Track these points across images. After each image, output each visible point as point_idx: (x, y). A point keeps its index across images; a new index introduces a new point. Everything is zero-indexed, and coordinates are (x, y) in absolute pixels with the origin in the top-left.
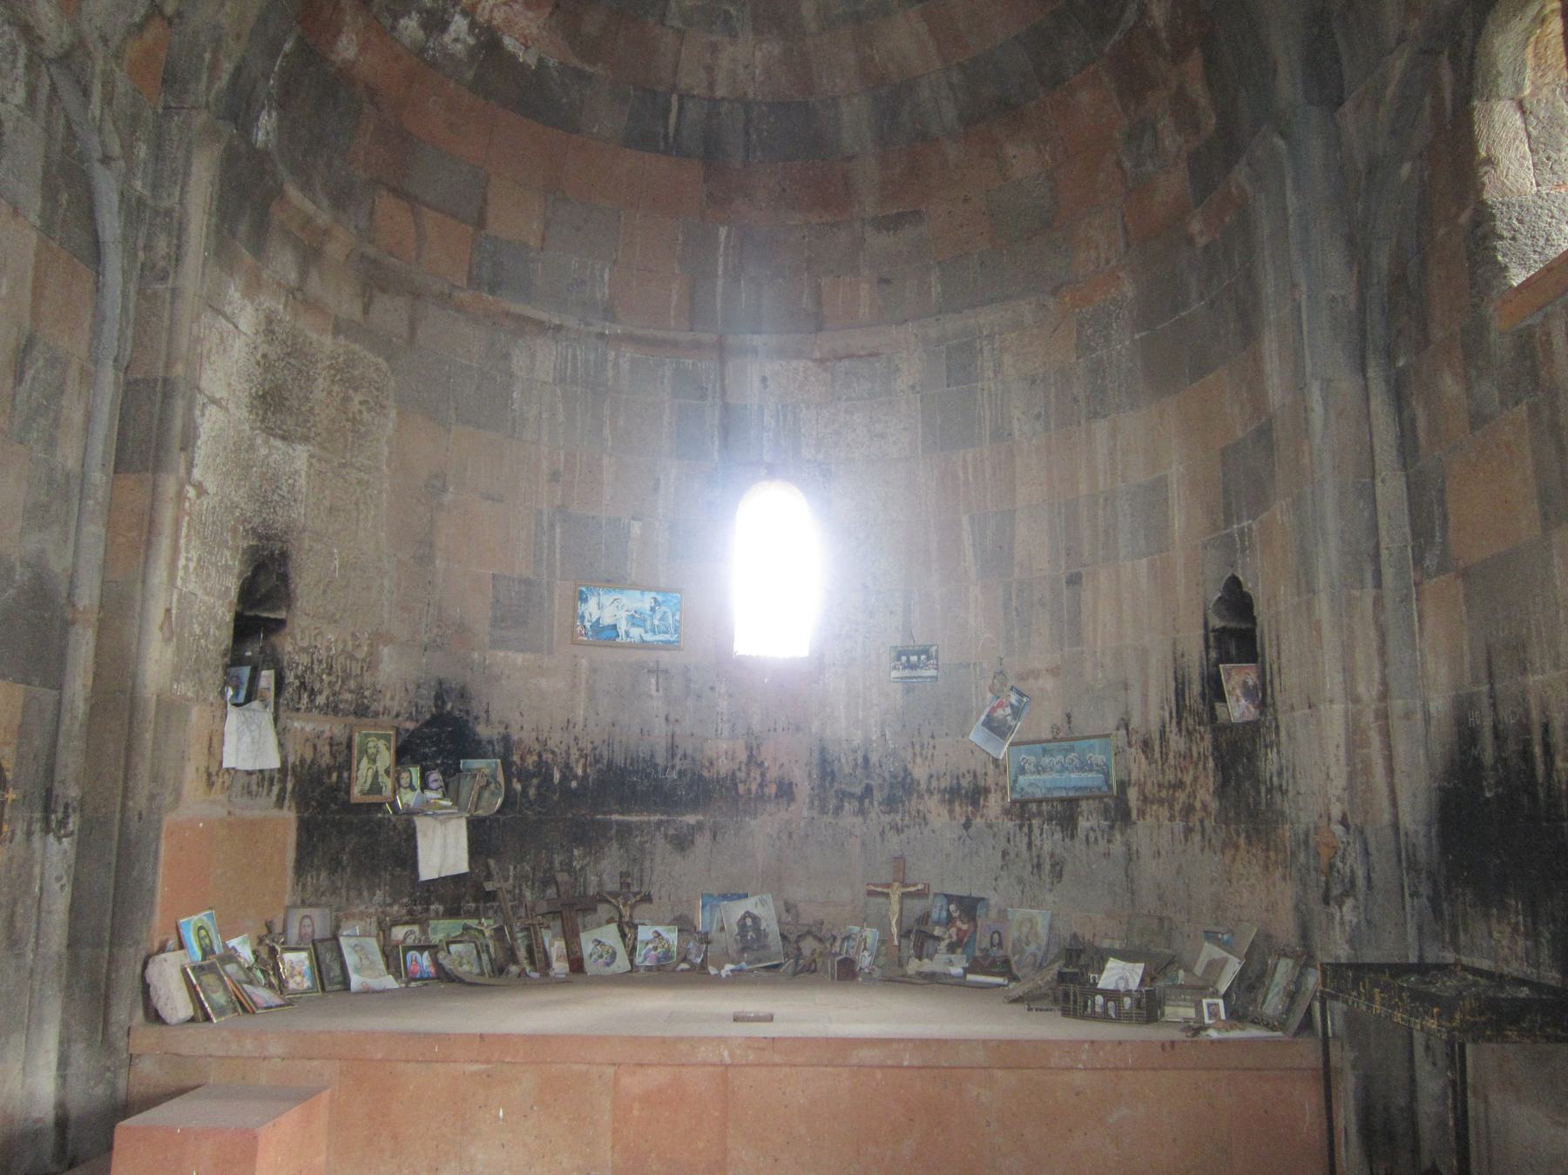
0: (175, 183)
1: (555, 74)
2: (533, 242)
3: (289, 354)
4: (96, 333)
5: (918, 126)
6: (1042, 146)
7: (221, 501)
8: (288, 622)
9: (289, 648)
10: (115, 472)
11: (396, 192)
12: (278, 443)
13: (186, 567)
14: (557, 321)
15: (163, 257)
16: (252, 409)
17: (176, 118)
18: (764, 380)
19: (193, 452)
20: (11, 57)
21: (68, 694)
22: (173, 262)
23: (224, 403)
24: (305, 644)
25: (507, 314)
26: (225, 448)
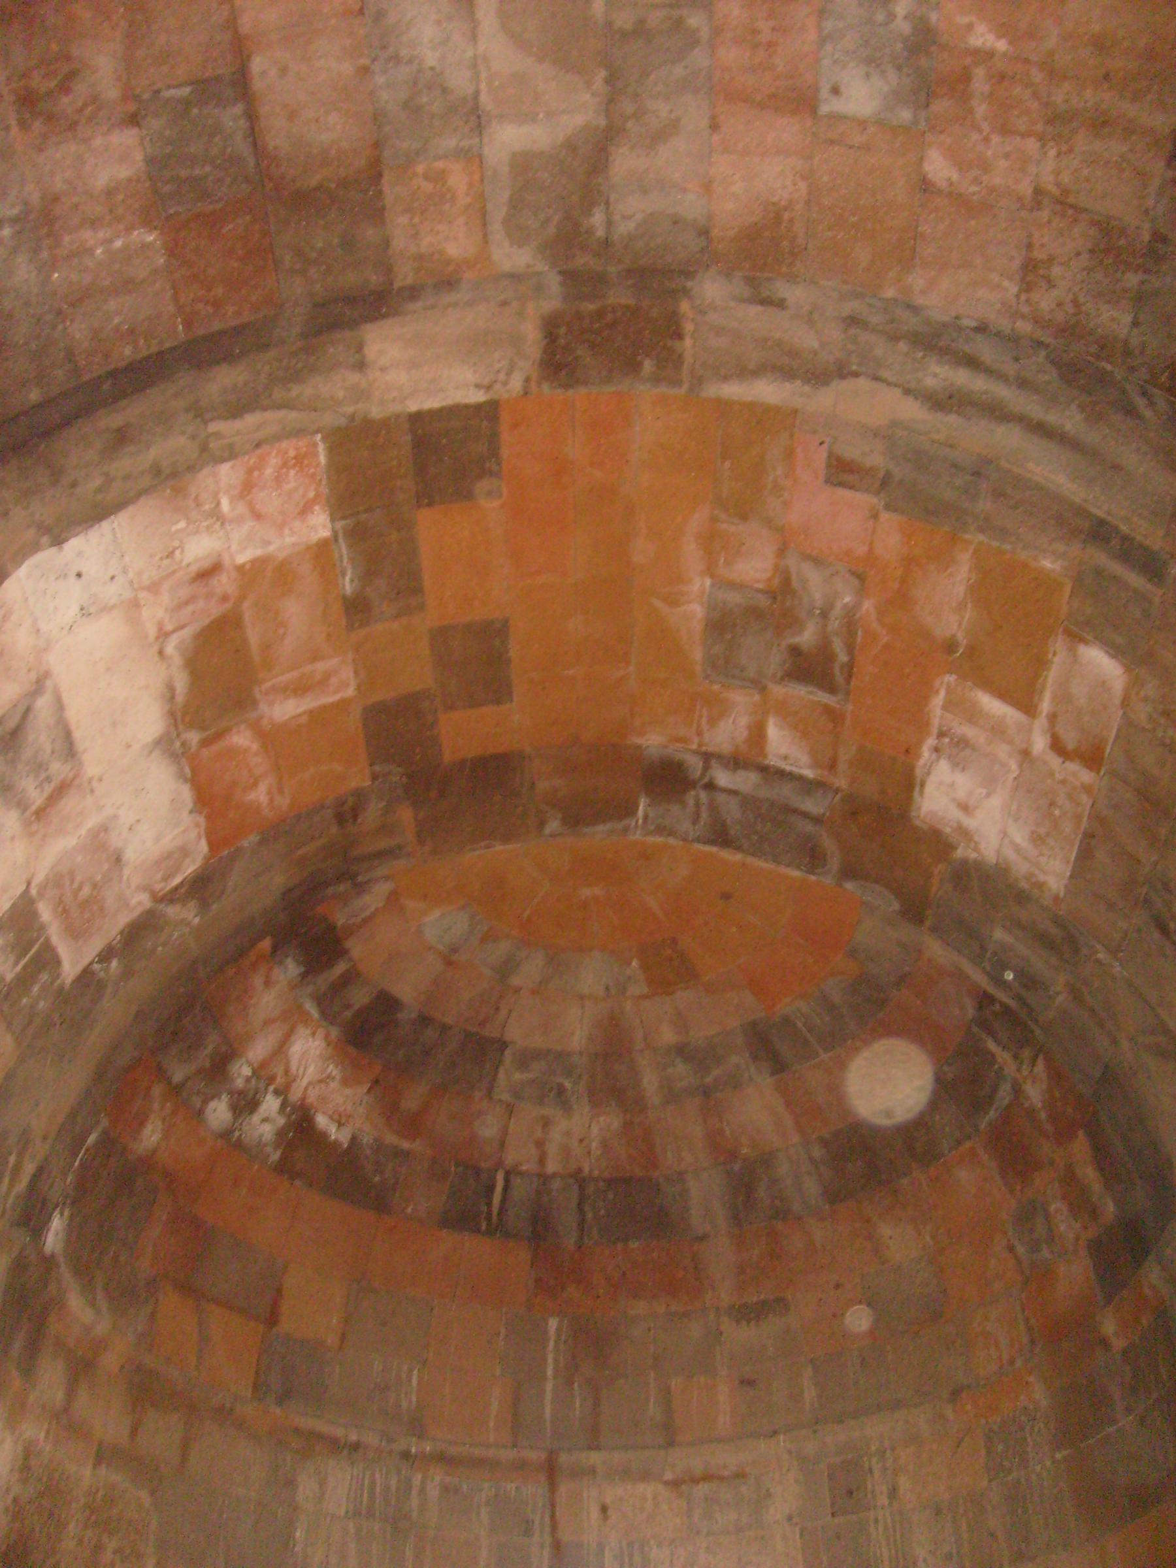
1: (368, 1152)
2: (332, 1340)
5: (777, 1203)
6: (921, 1227)
11: (186, 1288)
14: (353, 1437)
18: (604, 1509)
25: (297, 1430)
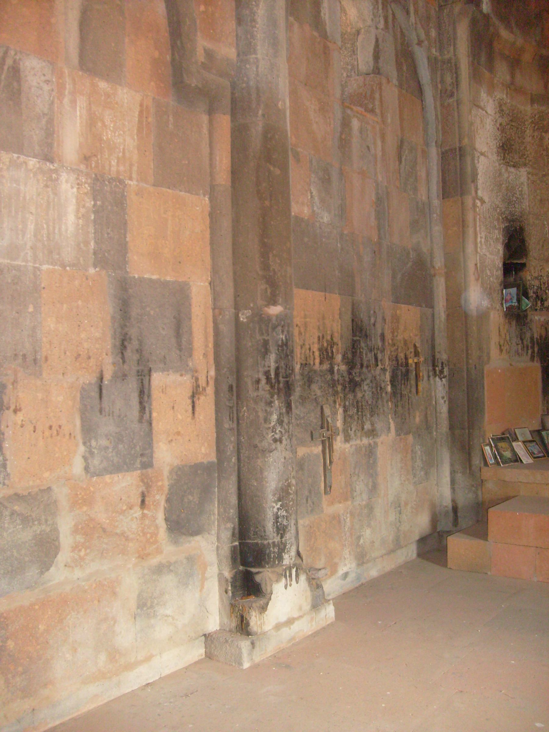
0: (450, 45)
3: (511, 121)
4: (425, 130)
7: (491, 206)
8: (527, 265)
9: (529, 278)
10: (443, 199)
12: (512, 170)
13: (481, 242)
15: (450, 85)
16: (498, 153)
17: (445, 11)
19: (477, 182)
20: (376, 6)
21: (436, 310)
22: (455, 86)
23: (486, 154)
24: (536, 275)
26: (490, 177)
